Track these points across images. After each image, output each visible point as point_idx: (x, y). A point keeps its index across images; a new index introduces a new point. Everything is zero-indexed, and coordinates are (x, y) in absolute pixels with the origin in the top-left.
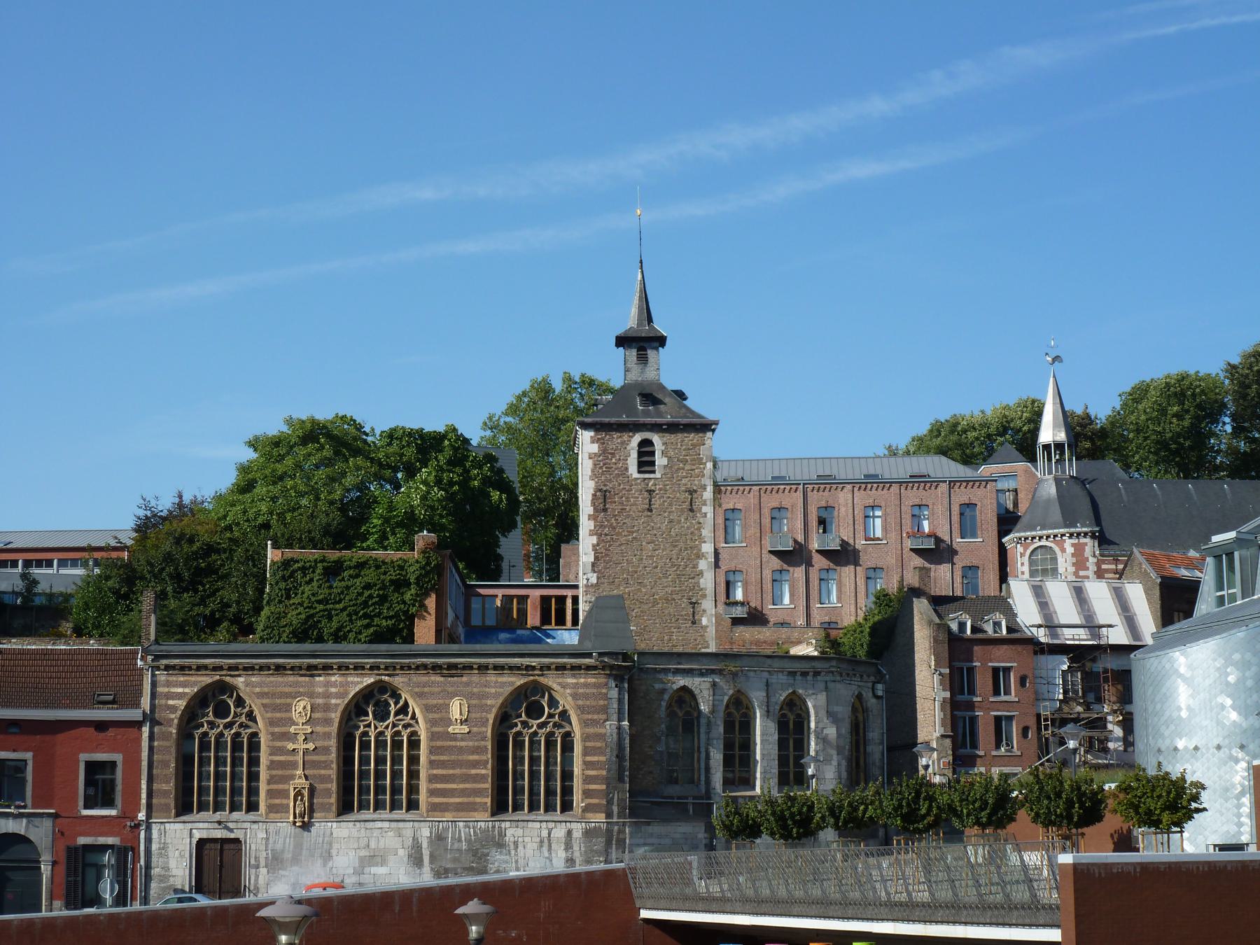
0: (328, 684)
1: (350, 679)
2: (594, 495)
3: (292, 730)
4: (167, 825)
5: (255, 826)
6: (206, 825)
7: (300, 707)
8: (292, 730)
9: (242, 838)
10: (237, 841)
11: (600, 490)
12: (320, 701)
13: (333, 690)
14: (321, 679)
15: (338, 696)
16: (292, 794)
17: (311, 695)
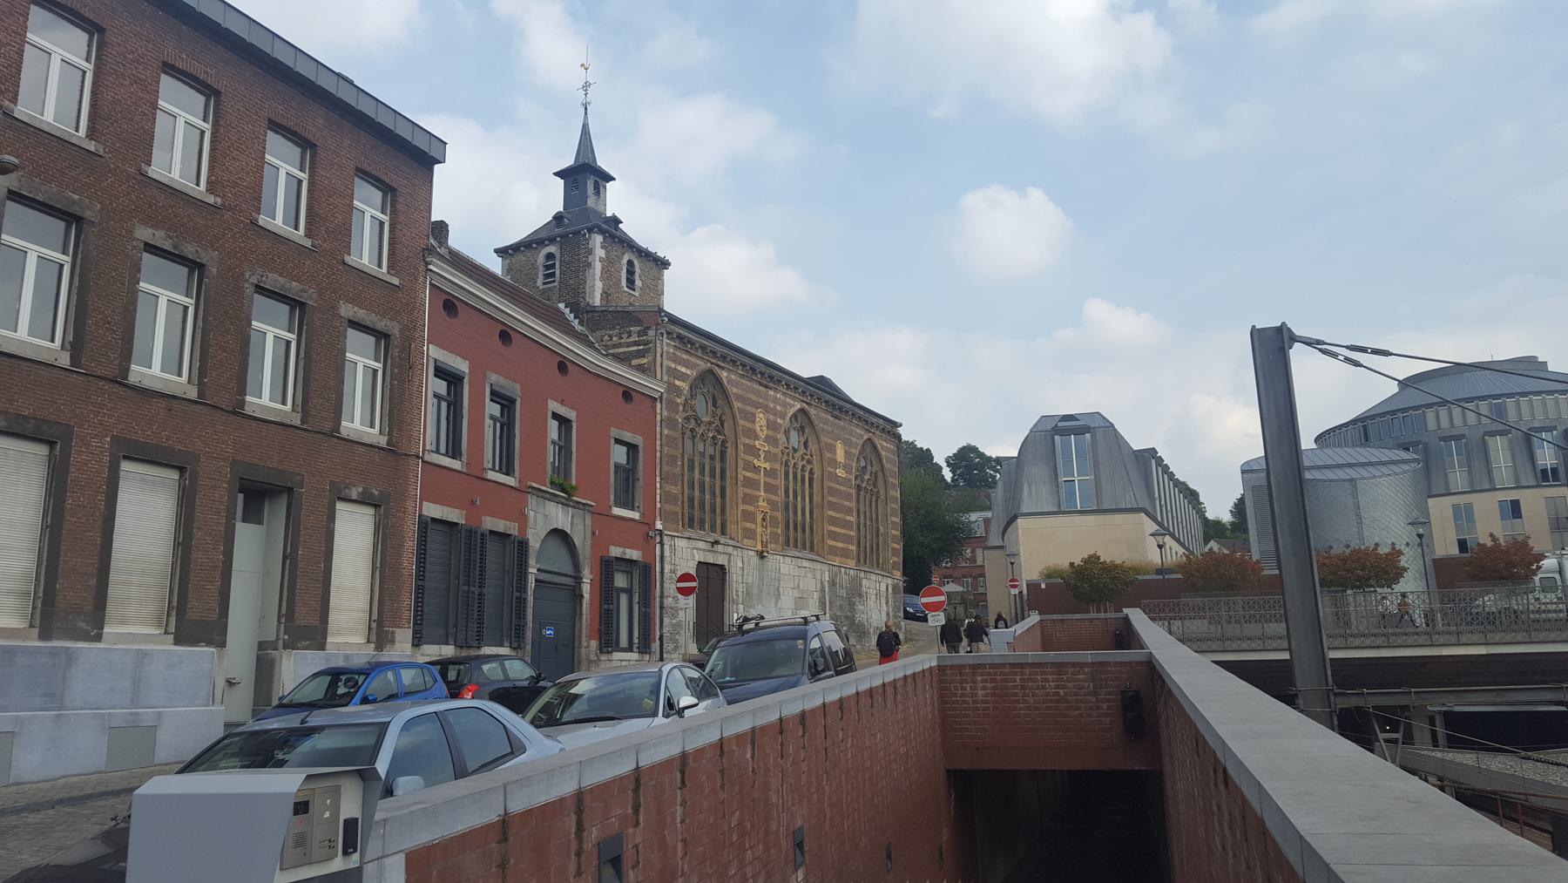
0: (776, 401)
1: (788, 400)
2: (602, 295)
3: (757, 443)
4: (676, 539)
5: (735, 553)
6: (701, 545)
7: (761, 419)
8: (757, 443)
9: (726, 564)
10: (722, 567)
11: (605, 293)
12: (771, 417)
13: (779, 408)
14: (772, 393)
15: (783, 417)
16: (759, 517)
17: (766, 410)
